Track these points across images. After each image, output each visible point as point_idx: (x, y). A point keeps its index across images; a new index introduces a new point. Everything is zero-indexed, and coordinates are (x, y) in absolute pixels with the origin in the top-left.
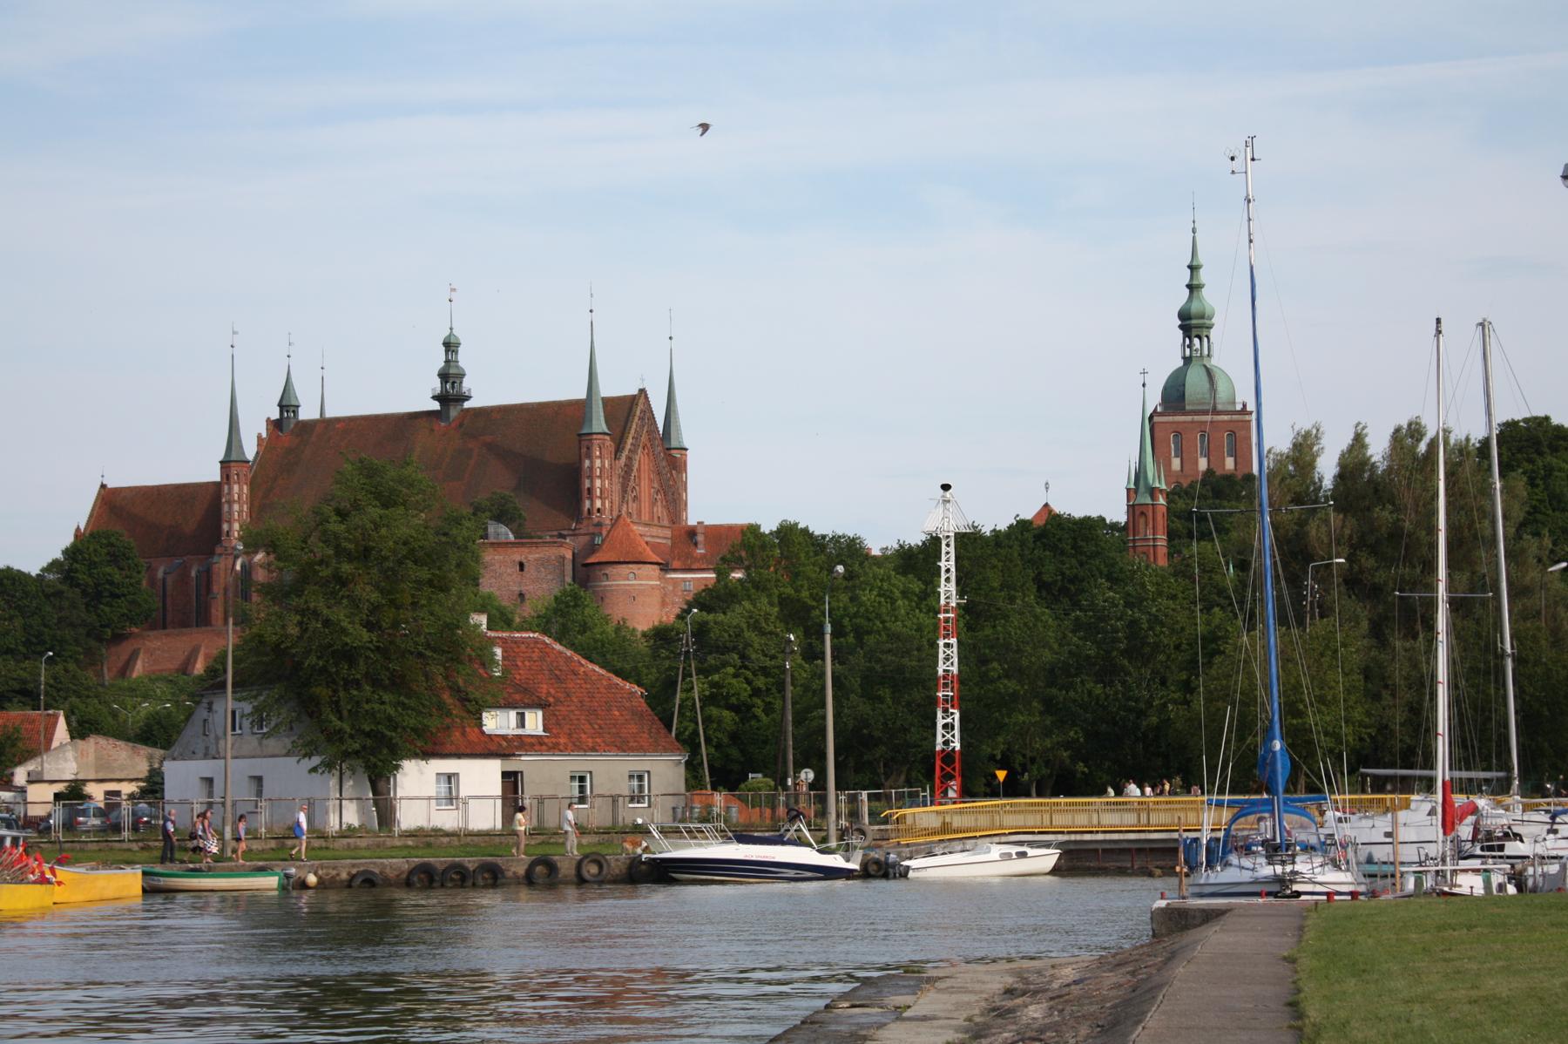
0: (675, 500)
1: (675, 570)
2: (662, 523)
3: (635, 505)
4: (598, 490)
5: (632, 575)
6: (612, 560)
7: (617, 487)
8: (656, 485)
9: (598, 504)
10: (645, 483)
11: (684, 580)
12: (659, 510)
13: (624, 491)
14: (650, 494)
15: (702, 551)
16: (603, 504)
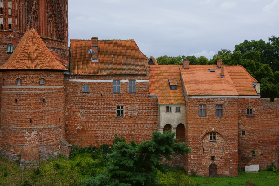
0: (61, 22)
1: (76, 76)
2: (53, 38)
3: (36, 24)
4: (10, 10)
5: (42, 81)
6: (25, 68)
7: (23, 10)
8: (49, 11)
9: (10, 21)
10: (42, 9)
11: (83, 84)
12: (51, 28)
13: (29, 13)
14: (45, 16)
15: (96, 61)
16: (14, 22)
